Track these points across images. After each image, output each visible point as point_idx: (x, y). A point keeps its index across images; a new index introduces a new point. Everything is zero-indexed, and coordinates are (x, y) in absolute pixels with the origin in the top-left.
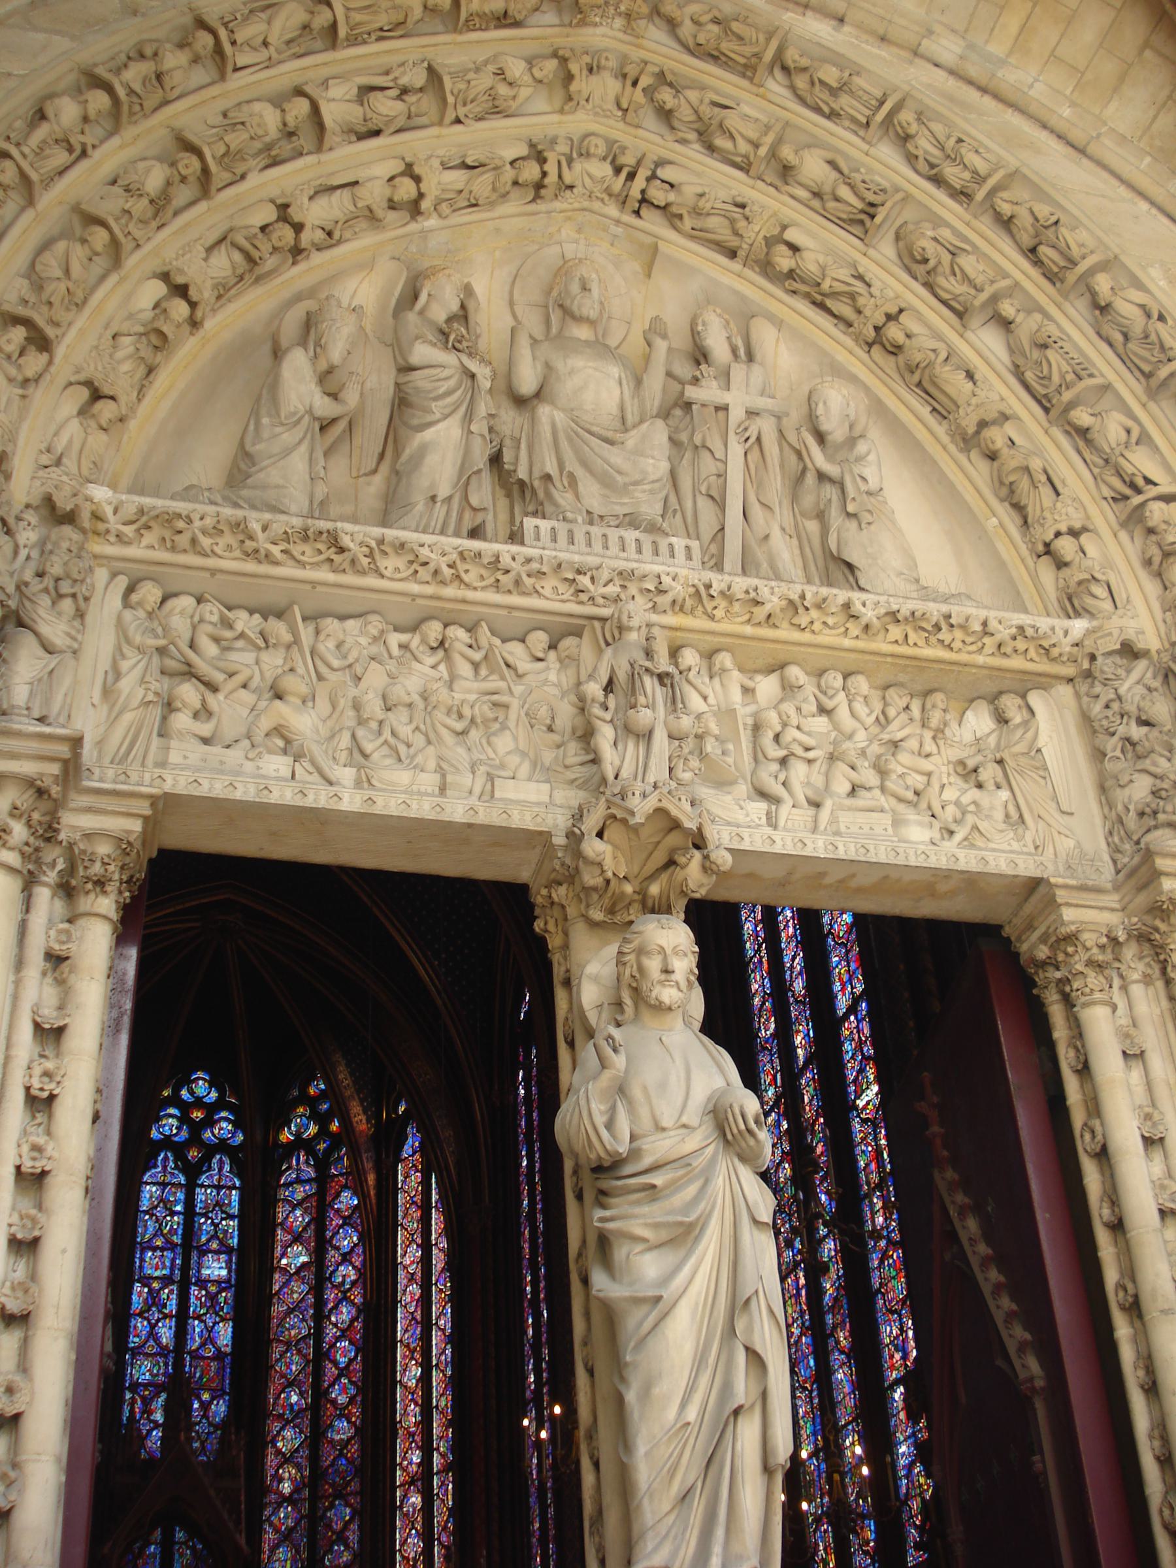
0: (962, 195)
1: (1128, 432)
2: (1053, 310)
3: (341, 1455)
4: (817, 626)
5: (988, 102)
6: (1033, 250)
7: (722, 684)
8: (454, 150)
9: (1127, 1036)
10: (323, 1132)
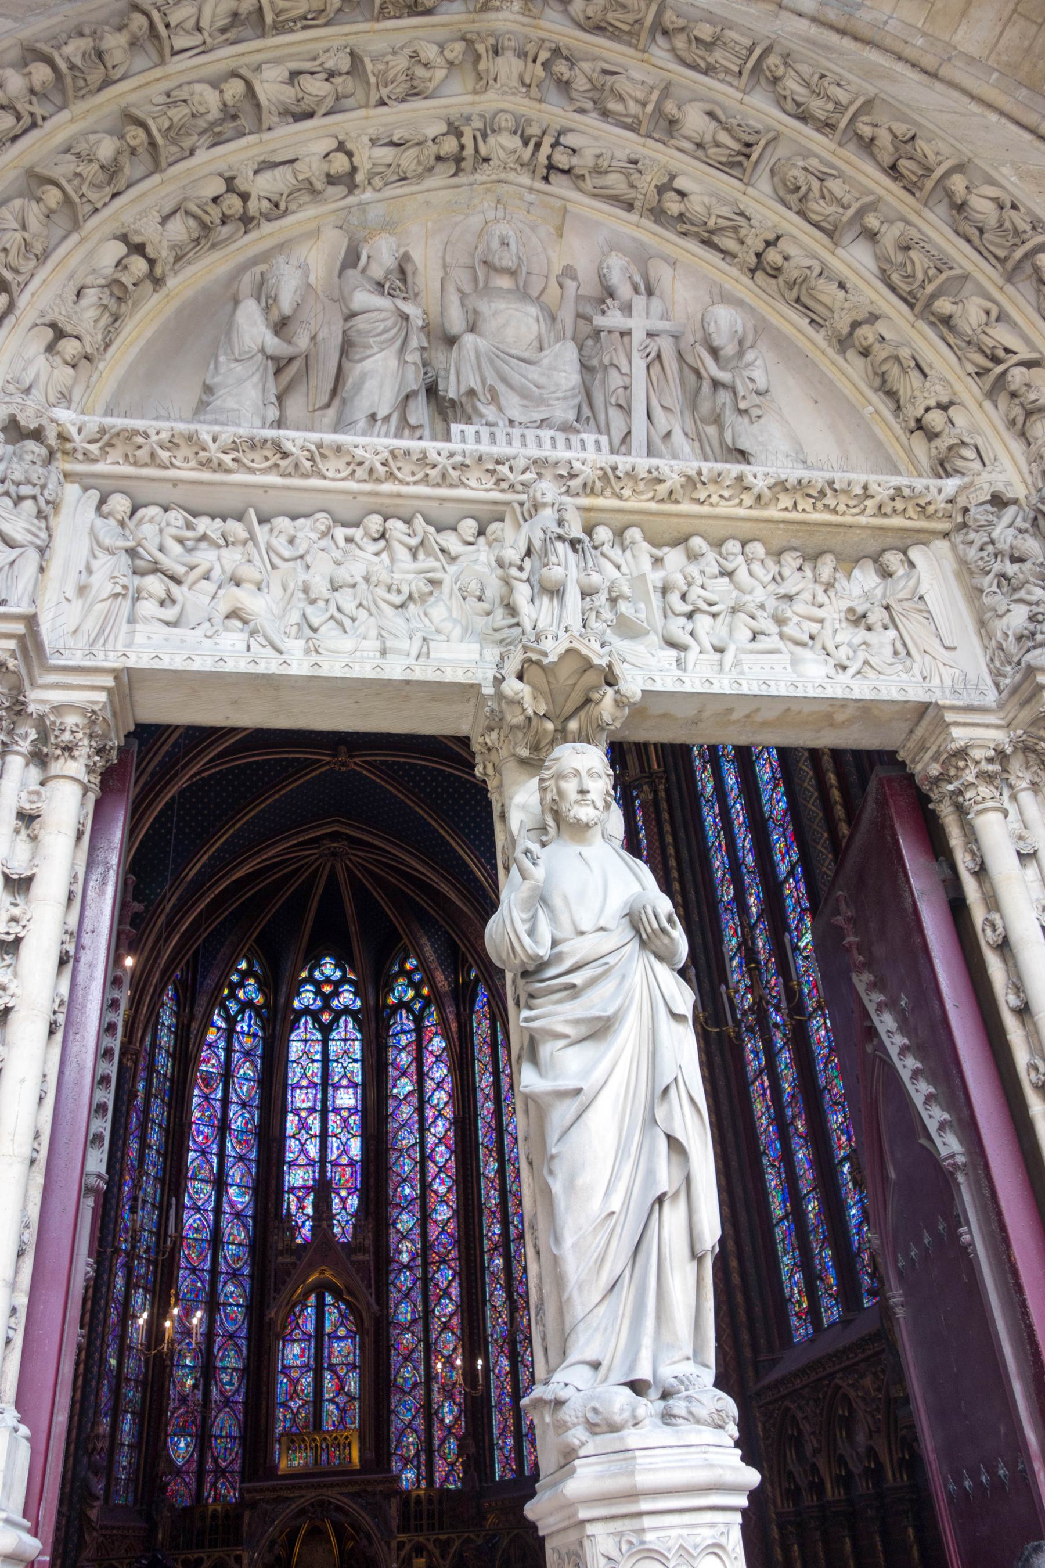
0: (827, 126)
1: (988, 313)
2: (913, 218)
4: (715, 499)
5: (847, 43)
6: (893, 167)
7: (634, 556)
8: (382, 129)
9: (1021, 838)
10: (418, 995)
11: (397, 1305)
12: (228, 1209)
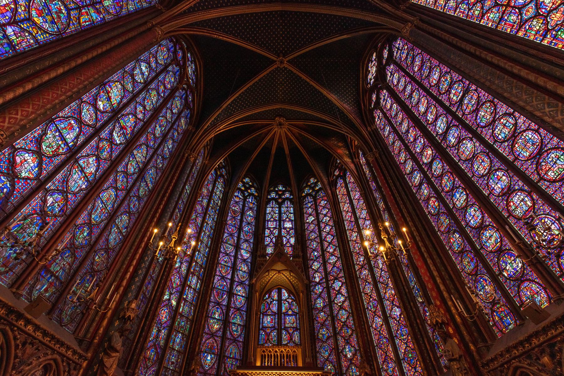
3: (334, 266)
10: (313, 190)
11: (316, 300)
12: (240, 257)
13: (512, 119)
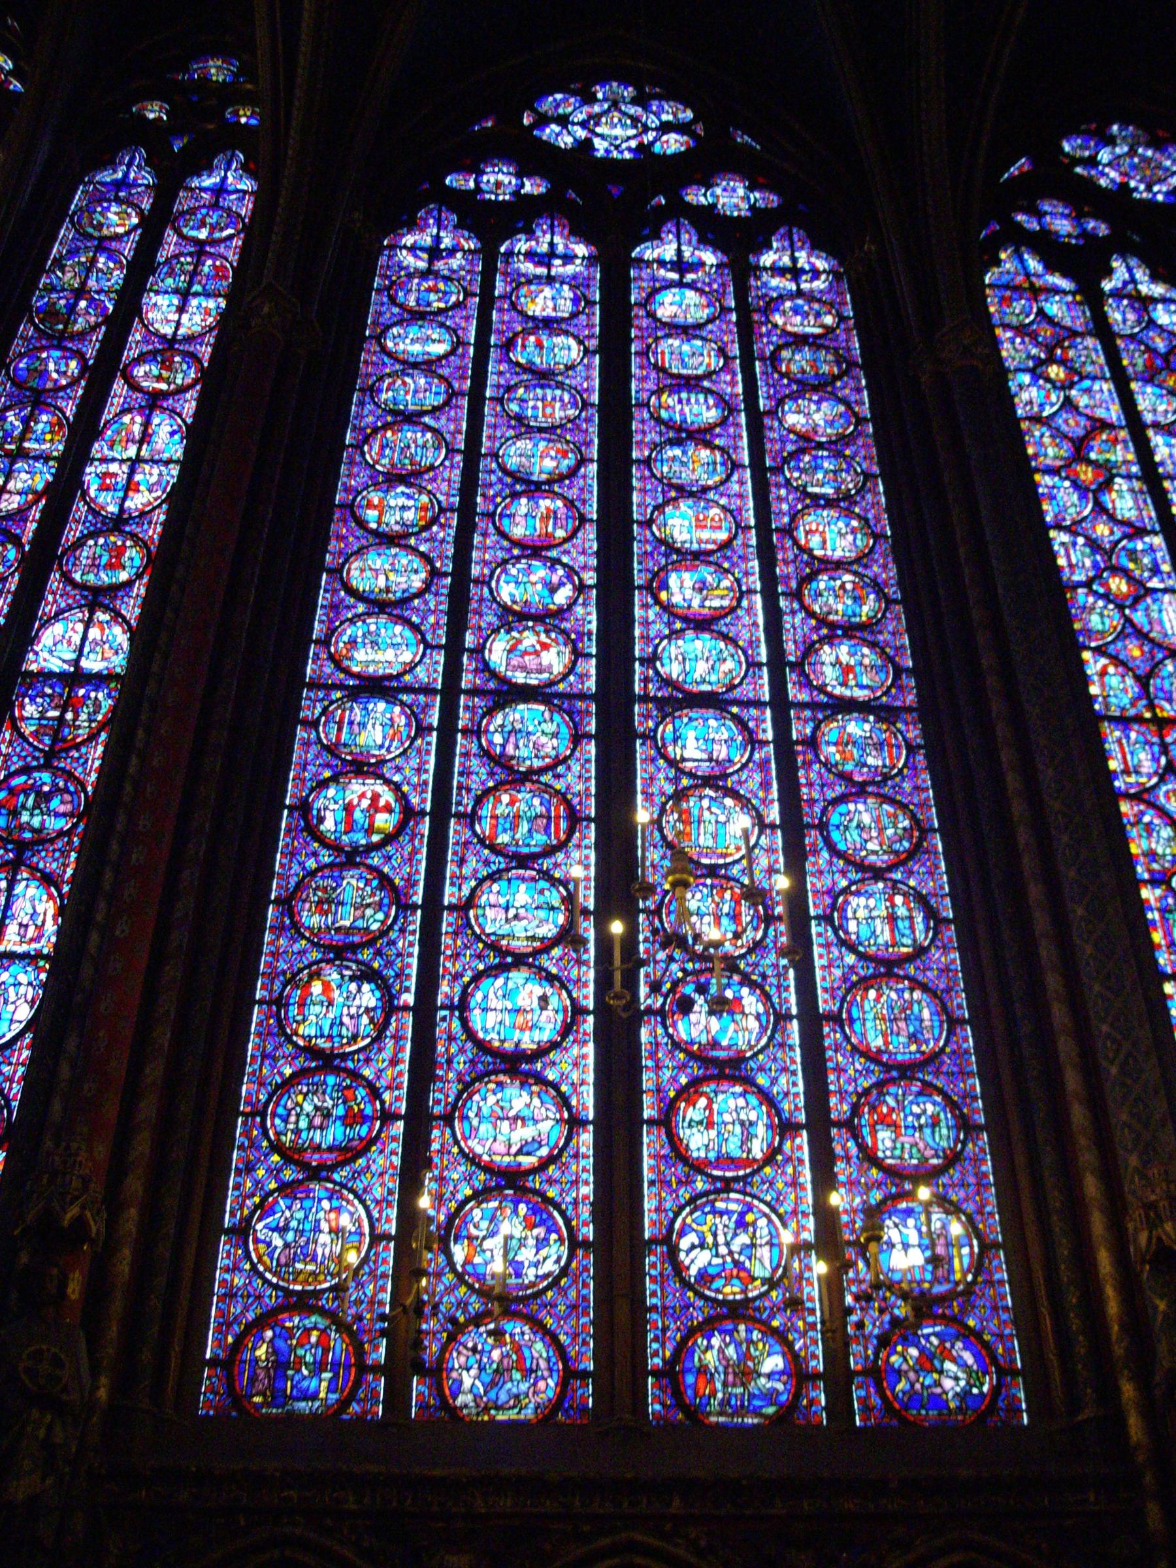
13: (927, 929)
